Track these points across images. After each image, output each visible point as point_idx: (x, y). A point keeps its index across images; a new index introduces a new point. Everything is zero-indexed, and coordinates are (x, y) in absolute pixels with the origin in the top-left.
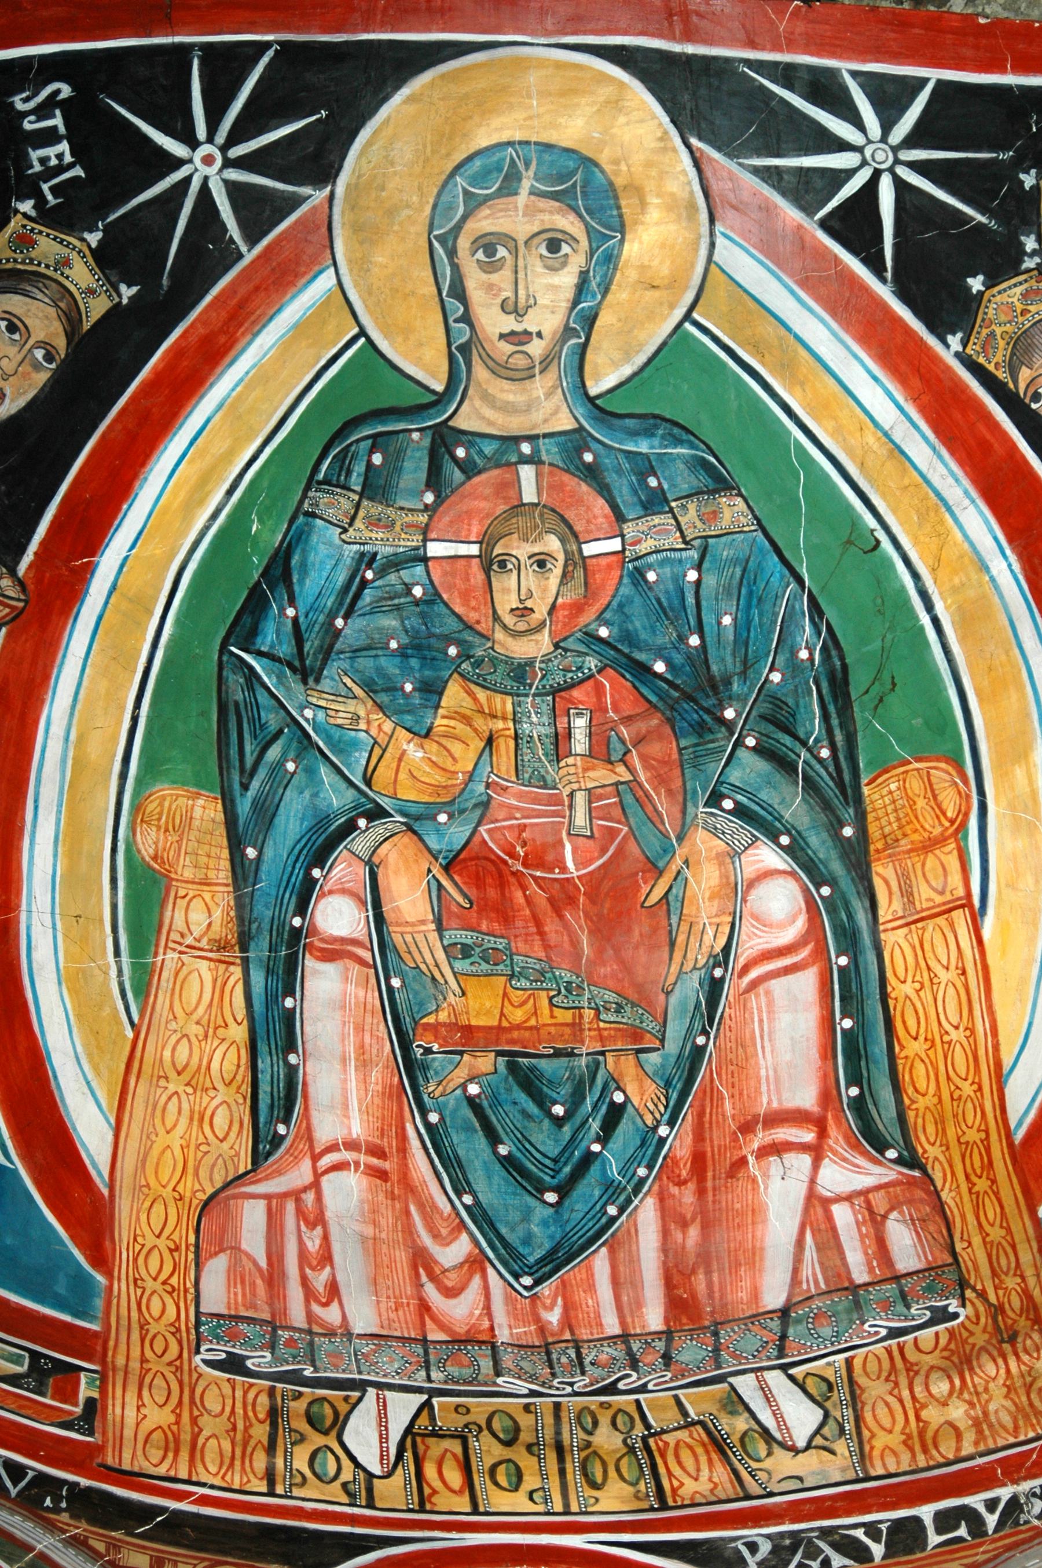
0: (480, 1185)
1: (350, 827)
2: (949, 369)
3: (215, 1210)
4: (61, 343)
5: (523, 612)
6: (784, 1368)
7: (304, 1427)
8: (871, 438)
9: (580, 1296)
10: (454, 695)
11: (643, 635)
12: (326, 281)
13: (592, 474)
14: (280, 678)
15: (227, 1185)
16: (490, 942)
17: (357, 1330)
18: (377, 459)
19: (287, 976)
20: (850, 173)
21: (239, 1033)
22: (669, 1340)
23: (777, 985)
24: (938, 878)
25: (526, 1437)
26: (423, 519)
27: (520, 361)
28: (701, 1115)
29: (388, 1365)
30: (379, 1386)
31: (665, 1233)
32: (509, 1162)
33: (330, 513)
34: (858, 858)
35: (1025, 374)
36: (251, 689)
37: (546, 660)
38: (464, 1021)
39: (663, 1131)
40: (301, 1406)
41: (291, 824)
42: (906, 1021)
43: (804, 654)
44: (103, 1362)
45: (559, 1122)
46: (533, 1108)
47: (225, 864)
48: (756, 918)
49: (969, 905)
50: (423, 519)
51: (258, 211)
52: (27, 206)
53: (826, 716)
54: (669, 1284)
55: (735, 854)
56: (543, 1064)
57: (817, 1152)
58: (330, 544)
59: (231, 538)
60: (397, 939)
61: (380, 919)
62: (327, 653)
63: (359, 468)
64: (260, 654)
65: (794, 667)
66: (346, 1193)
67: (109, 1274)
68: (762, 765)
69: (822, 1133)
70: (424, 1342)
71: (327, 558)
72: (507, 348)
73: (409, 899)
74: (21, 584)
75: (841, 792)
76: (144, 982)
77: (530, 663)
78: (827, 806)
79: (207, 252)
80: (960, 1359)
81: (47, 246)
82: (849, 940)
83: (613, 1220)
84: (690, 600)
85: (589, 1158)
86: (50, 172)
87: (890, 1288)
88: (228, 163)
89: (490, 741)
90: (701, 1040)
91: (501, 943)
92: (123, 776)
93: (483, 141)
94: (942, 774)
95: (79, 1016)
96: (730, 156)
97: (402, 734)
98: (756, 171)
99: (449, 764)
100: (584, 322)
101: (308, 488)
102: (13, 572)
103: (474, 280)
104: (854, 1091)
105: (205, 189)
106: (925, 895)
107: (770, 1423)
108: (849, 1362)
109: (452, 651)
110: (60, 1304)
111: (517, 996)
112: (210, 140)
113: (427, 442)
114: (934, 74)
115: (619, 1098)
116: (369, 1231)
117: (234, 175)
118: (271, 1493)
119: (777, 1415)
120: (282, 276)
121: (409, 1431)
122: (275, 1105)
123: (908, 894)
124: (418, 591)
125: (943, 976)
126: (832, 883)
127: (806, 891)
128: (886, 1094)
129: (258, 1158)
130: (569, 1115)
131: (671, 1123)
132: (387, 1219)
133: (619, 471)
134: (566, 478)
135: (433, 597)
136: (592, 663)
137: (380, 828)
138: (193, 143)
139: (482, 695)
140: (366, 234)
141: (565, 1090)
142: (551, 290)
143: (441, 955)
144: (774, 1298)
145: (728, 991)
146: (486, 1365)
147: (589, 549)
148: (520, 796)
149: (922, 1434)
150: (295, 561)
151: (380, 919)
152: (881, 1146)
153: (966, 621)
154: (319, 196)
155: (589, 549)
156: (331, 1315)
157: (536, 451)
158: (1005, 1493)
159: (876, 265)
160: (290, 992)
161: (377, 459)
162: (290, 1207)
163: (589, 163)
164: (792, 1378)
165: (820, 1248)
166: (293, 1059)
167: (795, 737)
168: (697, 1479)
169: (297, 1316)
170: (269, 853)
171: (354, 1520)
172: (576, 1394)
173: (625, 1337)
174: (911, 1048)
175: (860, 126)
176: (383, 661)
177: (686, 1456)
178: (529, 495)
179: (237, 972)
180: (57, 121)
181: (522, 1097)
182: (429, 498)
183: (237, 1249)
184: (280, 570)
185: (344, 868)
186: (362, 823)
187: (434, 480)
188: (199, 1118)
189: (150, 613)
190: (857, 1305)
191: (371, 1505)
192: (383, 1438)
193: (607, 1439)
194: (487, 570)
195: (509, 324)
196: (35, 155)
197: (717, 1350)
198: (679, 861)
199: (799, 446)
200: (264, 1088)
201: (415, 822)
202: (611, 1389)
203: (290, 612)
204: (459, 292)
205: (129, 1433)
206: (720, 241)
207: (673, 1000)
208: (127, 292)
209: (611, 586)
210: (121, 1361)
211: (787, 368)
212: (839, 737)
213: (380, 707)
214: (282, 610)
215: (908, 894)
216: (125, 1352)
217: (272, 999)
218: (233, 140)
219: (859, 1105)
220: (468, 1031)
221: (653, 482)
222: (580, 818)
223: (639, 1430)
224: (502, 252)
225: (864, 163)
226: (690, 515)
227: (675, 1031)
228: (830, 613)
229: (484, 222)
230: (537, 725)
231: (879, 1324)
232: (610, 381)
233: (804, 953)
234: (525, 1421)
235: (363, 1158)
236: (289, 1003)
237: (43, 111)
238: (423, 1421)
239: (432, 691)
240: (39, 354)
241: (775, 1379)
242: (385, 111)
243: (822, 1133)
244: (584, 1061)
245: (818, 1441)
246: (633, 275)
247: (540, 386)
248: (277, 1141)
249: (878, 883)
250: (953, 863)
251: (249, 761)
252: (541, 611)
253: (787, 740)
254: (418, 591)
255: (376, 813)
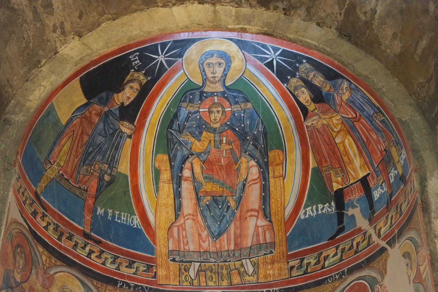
0: (208, 221)
1: (188, 157)
2: (284, 89)
3: (170, 230)
4: (139, 88)
5: (215, 120)
6: (250, 259)
7: (183, 271)
8: (272, 97)
9: (222, 242)
10: (204, 134)
11: (235, 124)
12: (182, 71)
13: (226, 98)
14: (177, 134)
15: (171, 225)
16: (210, 176)
17: (191, 250)
18: (191, 97)
19: (179, 185)
20: (269, 58)
21: (172, 196)
22: (234, 252)
23: (254, 186)
24: (279, 170)
25: (214, 271)
26: (199, 105)
27: (214, 81)
28: (241, 208)
29: (195, 257)
30: (194, 261)
31: (235, 230)
32: (212, 216)
33: (184, 106)
34: (267, 164)
35: (296, 93)
36: (172, 136)
37: (219, 127)
38: (206, 190)
39: (235, 211)
40: (183, 267)
41: (179, 158)
42: (272, 195)
43: (260, 129)
44: (156, 264)
45: (220, 209)
46: (216, 206)
47: (169, 166)
48: (251, 173)
49: (282, 176)
50: (199, 105)
51: (170, 63)
52: (133, 70)
53: (263, 140)
54: (235, 241)
55: (248, 162)
56: (218, 198)
57: (257, 217)
58: (184, 111)
59: (168, 112)
60: (196, 176)
61: (193, 173)
62: (184, 129)
63: (188, 98)
64: (173, 130)
65: (258, 132)
66: (189, 223)
67: (156, 246)
68: (253, 147)
69: (258, 214)
70: (200, 252)
71: (183, 113)
72: (212, 79)
73: (197, 169)
74: (135, 126)
75: (265, 154)
76: (157, 190)
77: (217, 128)
78: (263, 155)
79: (162, 69)
80: (273, 262)
81: (136, 75)
82: (265, 179)
83: (228, 227)
84: (242, 119)
85: (224, 215)
86: (136, 65)
87: (265, 245)
88: (165, 57)
89: (210, 141)
90: (242, 195)
91: (212, 176)
92: (153, 154)
93: (207, 50)
94: (280, 152)
95: (149, 198)
96: (249, 53)
97: (196, 141)
98: (253, 56)
99: (203, 145)
100: (225, 75)
101: (180, 102)
102: (134, 125)
103: (207, 69)
104: (264, 207)
105: (161, 62)
106: (277, 174)
107: (247, 270)
108: (258, 259)
109: (204, 126)
110: (150, 254)
111: (214, 186)
112: (162, 55)
113: (199, 94)
114: (282, 48)
115: (229, 204)
116: (192, 230)
117: (166, 59)
118: (180, 285)
119: (248, 268)
120: (175, 71)
121: (198, 270)
122: (178, 209)
123: (274, 172)
124: (198, 117)
125: (278, 188)
126: (263, 169)
127: (259, 170)
128: (268, 208)
129: (176, 219)
130: (222, 207)
131: (237, 210)
132: (195, 229)
133: (231, 98)
134: (222, 98)
135: (201, 118)
136: (226, 128)
137: (193, 157)
138: (159, 55)
139: (209, 134)
140: (188, 64)
141: (221, 203)
142: (219, 71)
143: (203, 179)
144: (249, 245)
145: (247, 186)
146: (209, 256)
147: (226, 110)
148: (215, 150)
149: (266, 275)
150: (178, 114)
151: (193, 173)
152: (266, 217)
153: (285, 128)
154: (180, 60)
155: (226, 110)
156: (187, 248)
157: (217, 94)
158: (275, 289)
159: (273, 71)
160: (180, 187)
161: (191, 97)
162: (181, 227)
163: (225, 53)
164: (250, 261)
165: (256, 236)
166: (180, 200)
167: (258, 143)
168: (236, 280)
169: (182, 249)
170: (176, 163)
171: (190, 288)
172: (221, 262)
173: (228, 250)
174: (272, 200)
175: (271, 52)
176: (193, 129)
177: (235, 275)
178: (216, 101)
179: (171, 185)
180: (137, 58)
181: (215, 204)
182: (200, 102)
183: (173, 236)
184: (176, 116)
185: (188, 164)
186: (190, 156)
187: (201, 99)
188: (167, 213)
189: (155, 126)
190: (260, 248)
191: (193, 286)
192: (194, 272)
193: (225, 272)
194: (209, 113)
195: (213, 75)
196: (133, 63)
197: (241, 254)
198: (239, 162)
199: (260, 96)
200: (176, 205)
201: (198, 155)
202: (225, 261)
203: (178, 122)
204: (204, 71)
205: (161, 277)
206: (247, 65)
207: (238, 187)
208: (149, 78)
209: (229, 115)
210: (159, 263)
211: (258, 84)
212: (265, 144)
213: (193, 137)
214: (176, 122)
215: (274, 172)
216: (159, 261)
217: (177, 189)
218: (165, 54)
219: (264, 209)
220: (207, 192)
221: (236, 100)
222: (224, 154)
223: (229, 270)
224: (211, 65)
225: (271, 57)
226: (242, 105)
227: (238, 192)
228: (264, 123)
229: (208, 61)
230: (217, 139)
231: (263, 252)
232: (229, 84)
233: (258, 180)
234: (214, 267)
235: (191, 217)
236: (180, 189)
237: (134, 57)
238: (200, 268)
239: (201, 133)
240: (136, 90)
241: (248, 260)
242: (191, 48)
243: (258, 214)
244: (224, 198)
245: (253, 274)
246: (233, 69)
247: (218, 84)
248: (179, 215)
249: (270, 170)
250: (281, 168)
251: (172, 148)
252: (218, 120)
253: (257, 143)
254: (198, 117)
255: (192, 154)
